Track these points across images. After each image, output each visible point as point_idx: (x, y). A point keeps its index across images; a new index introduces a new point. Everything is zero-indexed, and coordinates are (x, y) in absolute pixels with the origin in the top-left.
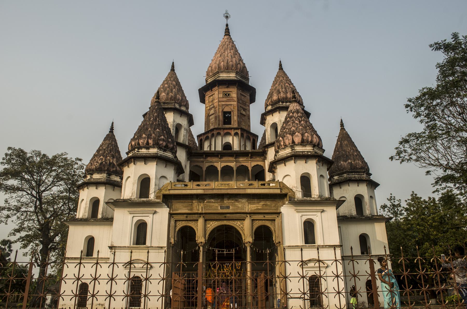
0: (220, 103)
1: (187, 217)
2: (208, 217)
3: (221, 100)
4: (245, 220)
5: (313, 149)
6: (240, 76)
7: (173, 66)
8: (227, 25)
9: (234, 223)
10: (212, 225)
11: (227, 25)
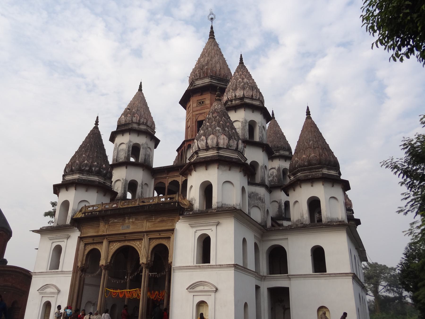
0: (194, 113)
1: (93, 239)
2: (111, 239)
3: (195, 109)
5: (218, 153)
6: (217, 80)
7: (141, 86)
8: (212, 28)
9: (133, 243)
11: (212, 28)
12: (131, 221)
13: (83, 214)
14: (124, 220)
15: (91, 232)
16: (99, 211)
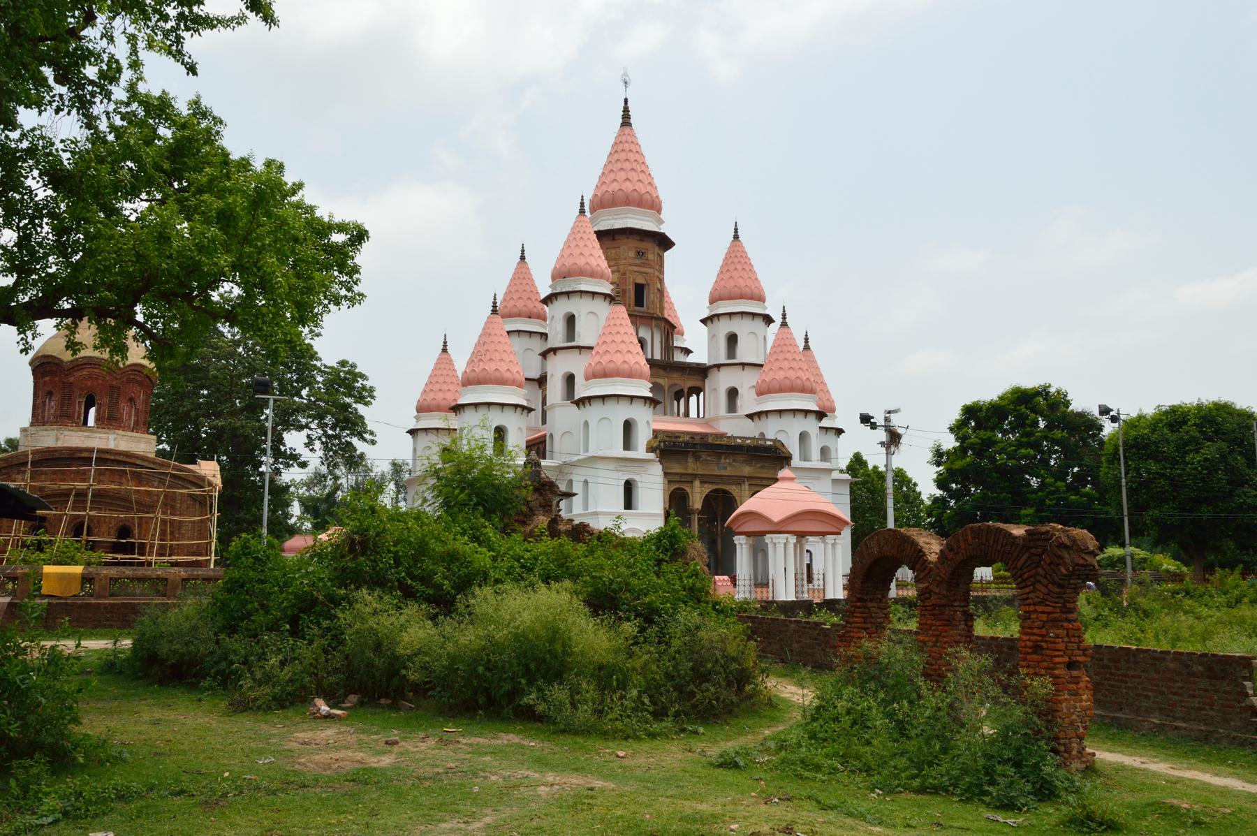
0: (630, 268)
3: (632, 261)
4: (740, 484)
8: (626, 101)
10: (708, 488)
11: (626, 101)
12: (728, 461)
13: (662, 444)
14: (720, 459)
15: (677, 468)
16: (684, 442)
